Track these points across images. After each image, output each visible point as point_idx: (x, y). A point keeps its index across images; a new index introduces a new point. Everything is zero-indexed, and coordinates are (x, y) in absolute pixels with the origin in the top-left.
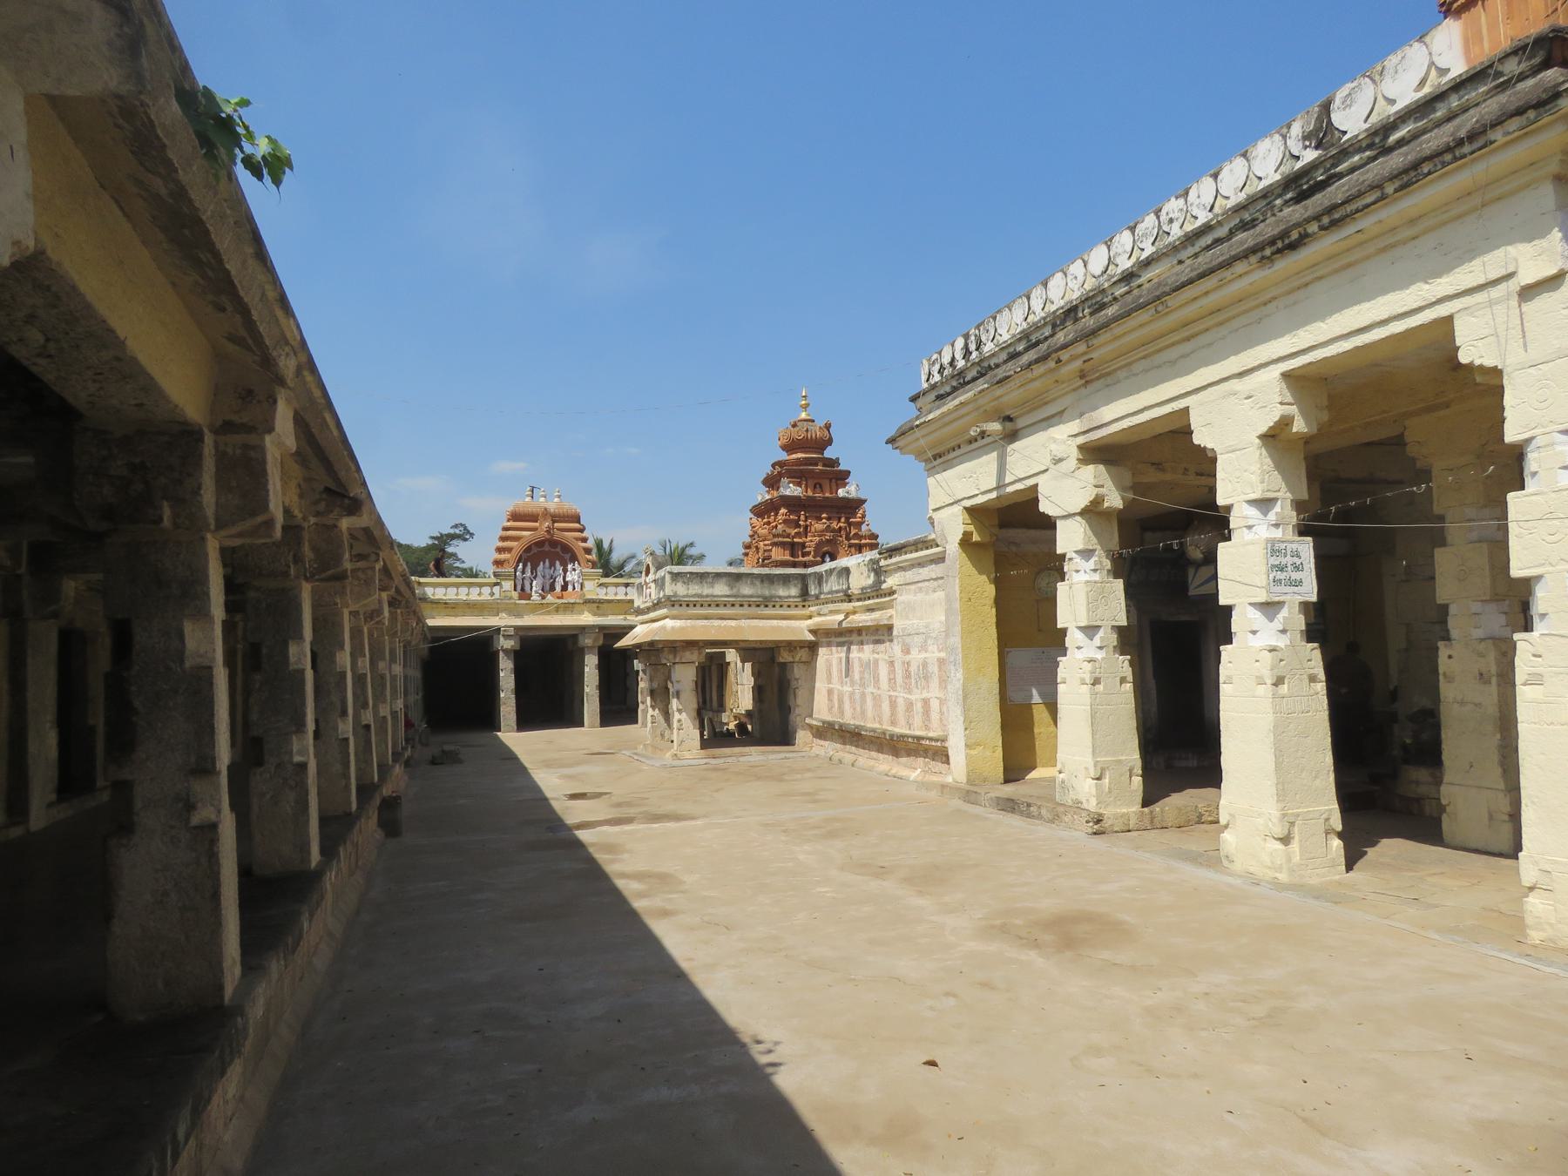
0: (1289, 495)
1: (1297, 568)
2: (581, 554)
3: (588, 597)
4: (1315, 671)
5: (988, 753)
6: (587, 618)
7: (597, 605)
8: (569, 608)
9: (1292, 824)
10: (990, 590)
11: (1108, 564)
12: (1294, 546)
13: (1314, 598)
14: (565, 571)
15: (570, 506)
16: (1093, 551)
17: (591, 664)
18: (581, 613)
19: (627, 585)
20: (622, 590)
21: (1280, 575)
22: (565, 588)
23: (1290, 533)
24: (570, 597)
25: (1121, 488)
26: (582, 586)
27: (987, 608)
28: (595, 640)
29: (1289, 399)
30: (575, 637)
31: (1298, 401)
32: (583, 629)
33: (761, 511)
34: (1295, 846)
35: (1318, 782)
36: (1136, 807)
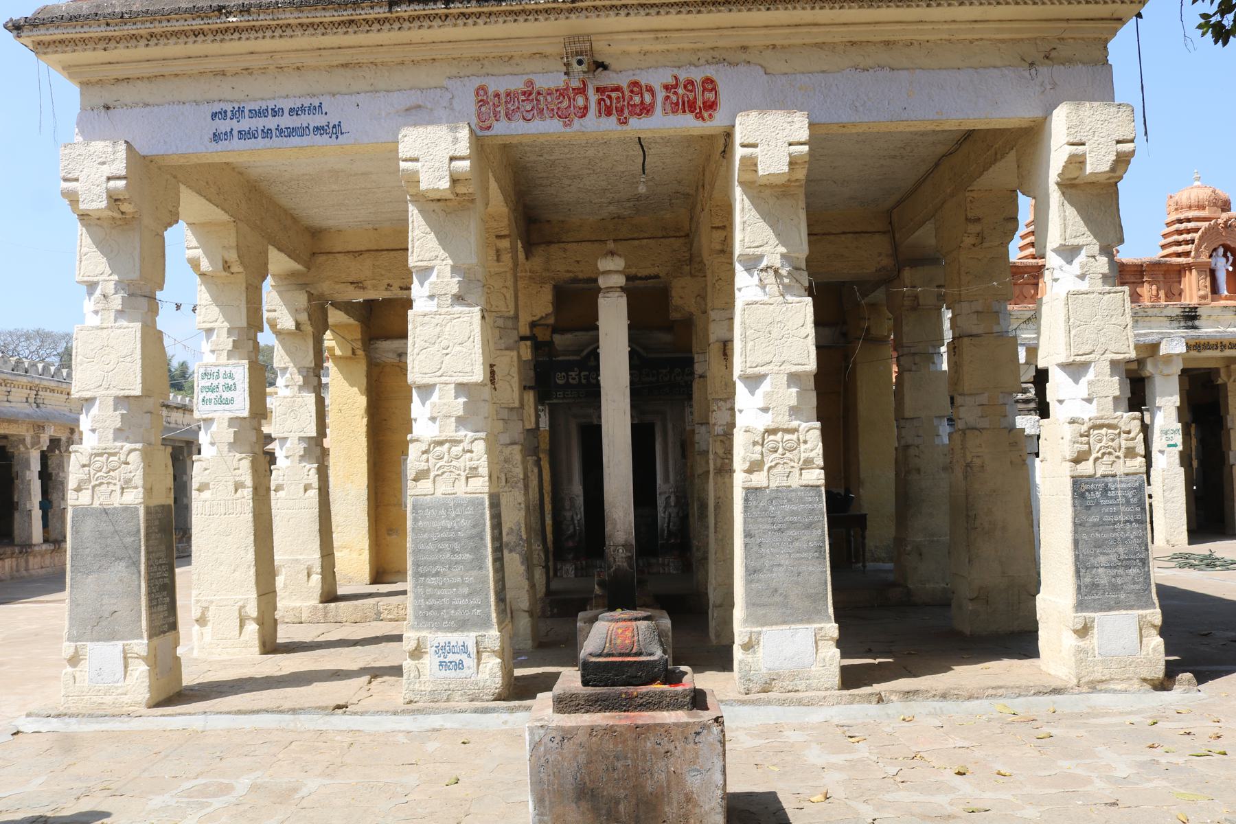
0: (226, 324)
1: (228, 388)
4: (242, 478)
5: (355, 555)
9: (207, 608)
10: (362, 401)
11: (300, 380)
12: (228, 369)
13: (246, 414)
16: (286, 368)
21: (210, 395)
23: (223, 358)
25: (295, 311)
27: (358, 418)
29: (195, 243)
31: (203, 245)
34: (207, 630)
35: (237, 574)
36: (314, 600)
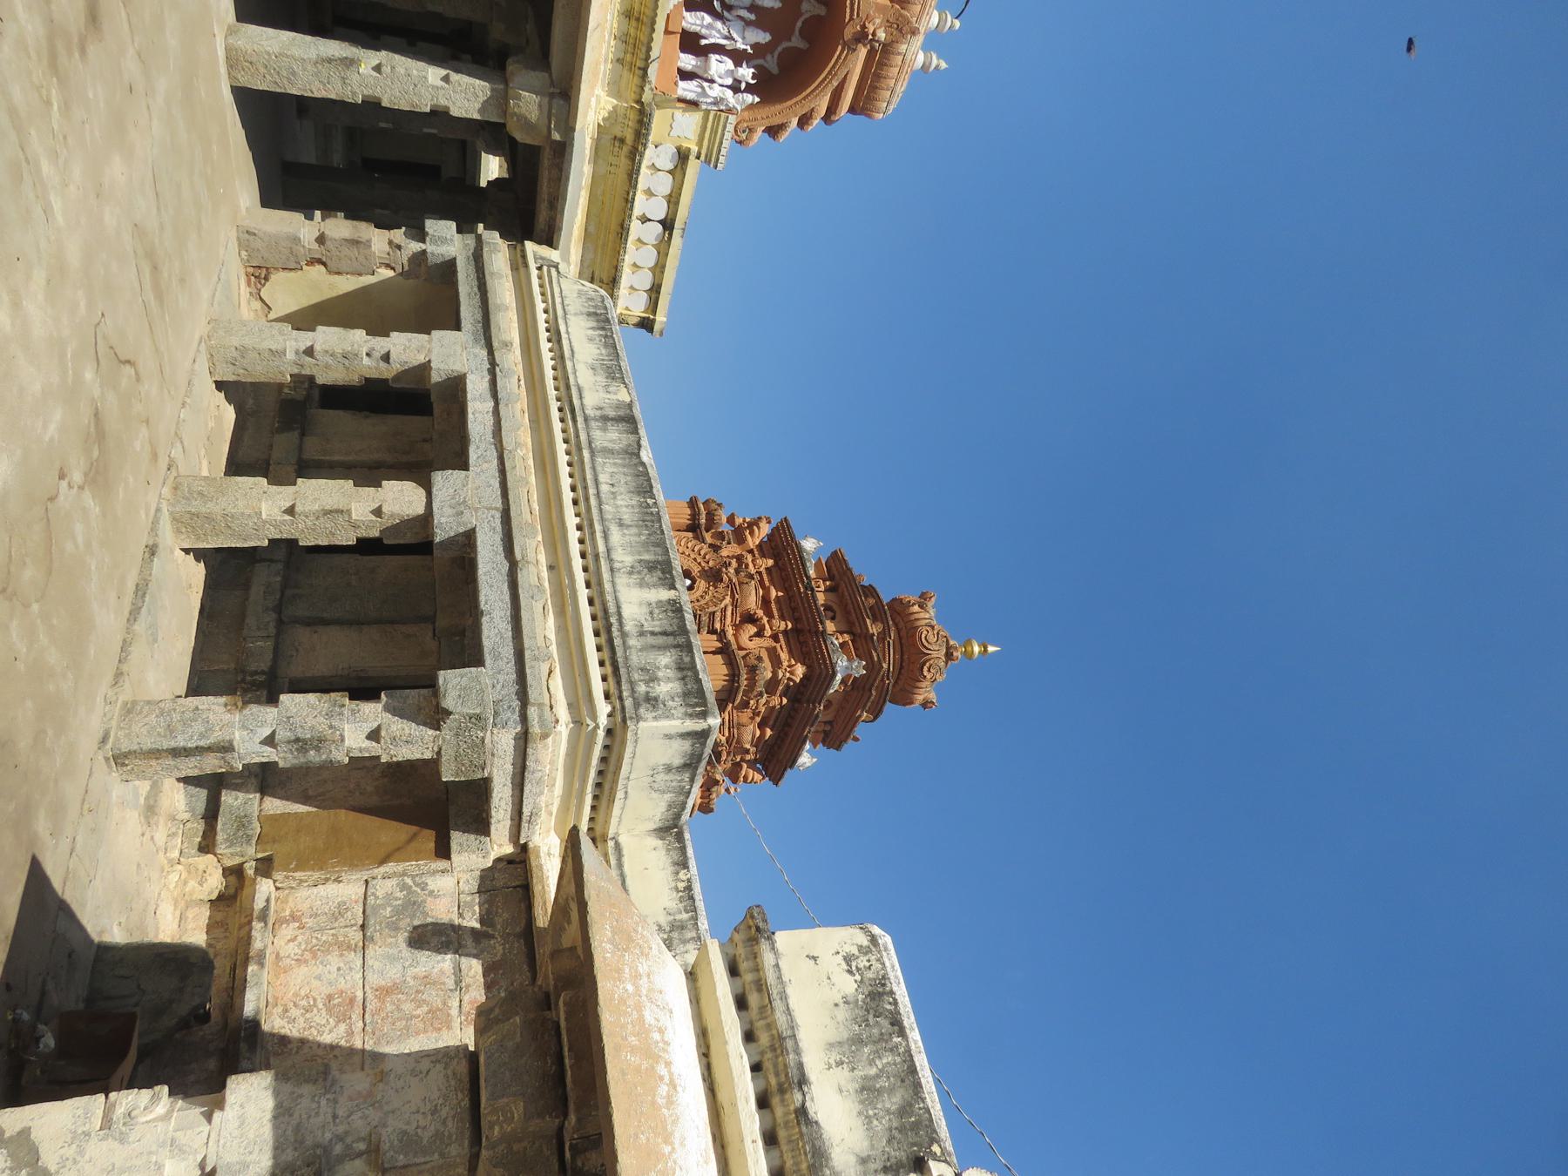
2: (774, 113)
3: (659, 119)
6: (596, 103)
7: (628, 140)
8: (634, 56)
14: (738, 57)
15: (895, 93)
17: (460, 93)
18: (615, 89)
19: (668, 224)
20: (659, 210)
22: (690, 42)
24: (665, 54)
26: (693, 104)
28: (528, 126)
30: (542, 59)
32: (564, 93)
33: (781, 545)
